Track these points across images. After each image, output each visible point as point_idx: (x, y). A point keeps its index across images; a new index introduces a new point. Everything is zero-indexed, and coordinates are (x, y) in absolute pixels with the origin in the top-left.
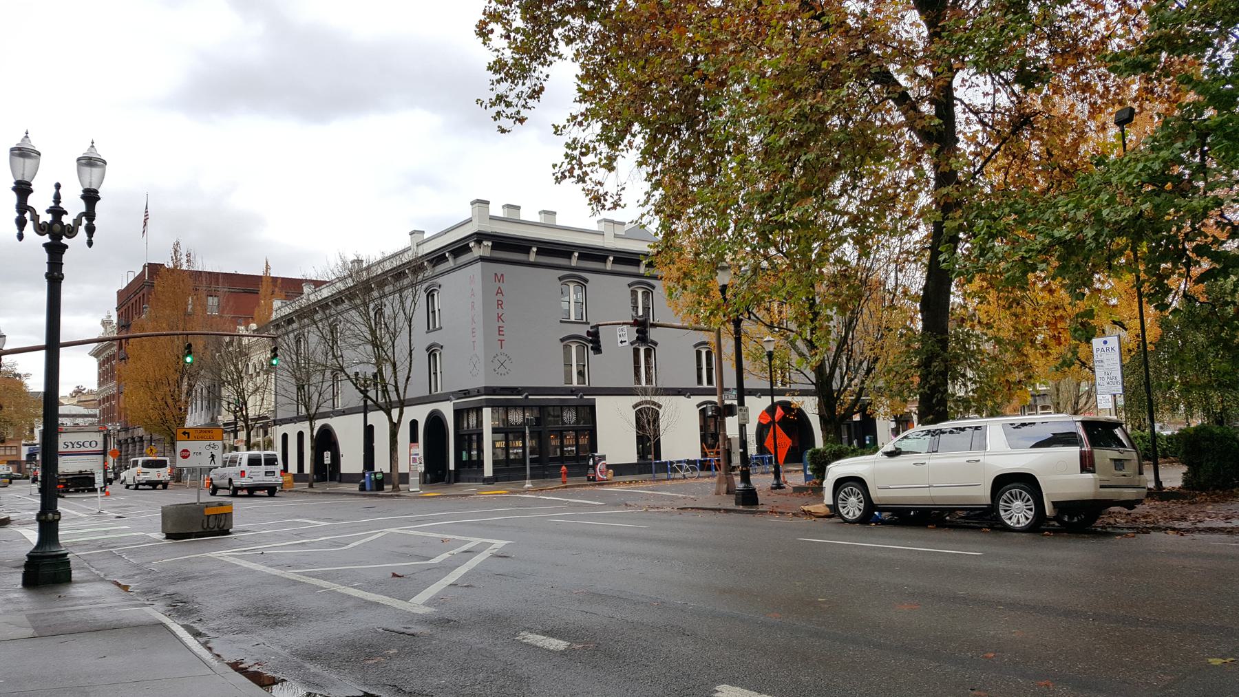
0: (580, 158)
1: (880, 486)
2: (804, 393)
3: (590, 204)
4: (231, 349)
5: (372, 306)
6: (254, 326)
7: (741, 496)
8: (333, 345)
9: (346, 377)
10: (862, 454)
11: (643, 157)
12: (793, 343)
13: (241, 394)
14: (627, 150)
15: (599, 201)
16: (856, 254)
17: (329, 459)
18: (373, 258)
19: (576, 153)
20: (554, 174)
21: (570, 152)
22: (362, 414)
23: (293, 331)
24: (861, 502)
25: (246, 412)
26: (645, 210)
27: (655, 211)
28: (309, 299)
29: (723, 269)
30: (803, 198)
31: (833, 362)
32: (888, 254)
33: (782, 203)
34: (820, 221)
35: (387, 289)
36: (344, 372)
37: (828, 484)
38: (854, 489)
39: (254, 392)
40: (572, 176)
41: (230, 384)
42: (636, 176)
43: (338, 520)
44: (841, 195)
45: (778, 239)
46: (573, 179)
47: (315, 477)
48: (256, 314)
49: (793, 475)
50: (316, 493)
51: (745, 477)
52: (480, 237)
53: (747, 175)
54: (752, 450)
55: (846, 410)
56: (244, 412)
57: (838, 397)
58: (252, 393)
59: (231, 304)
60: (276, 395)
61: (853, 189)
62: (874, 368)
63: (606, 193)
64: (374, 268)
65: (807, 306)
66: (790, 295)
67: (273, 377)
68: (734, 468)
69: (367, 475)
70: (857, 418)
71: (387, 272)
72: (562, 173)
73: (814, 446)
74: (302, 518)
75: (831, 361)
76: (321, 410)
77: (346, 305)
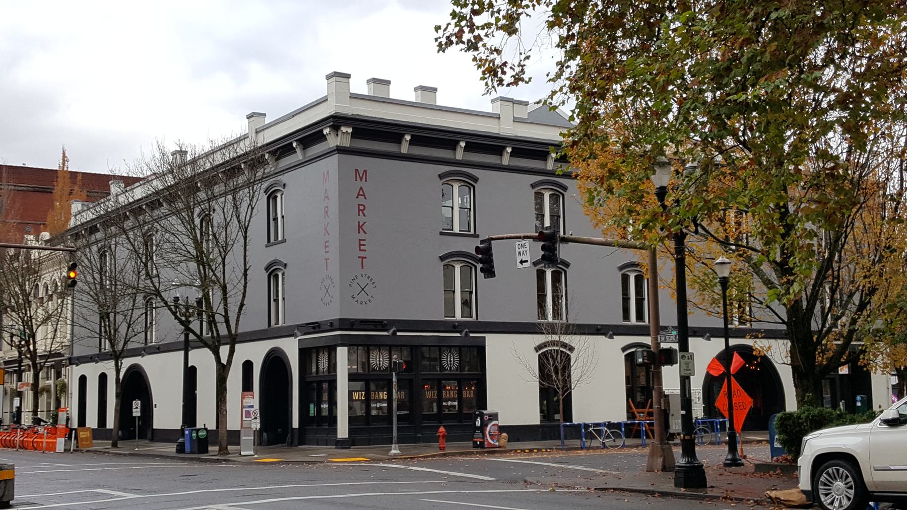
0: (471, 18)
1: (877, 466)
2: (771, 335)
3: (483, 79)
4: (15, 265)
5: (197, 210)
6: (46, 235)
7: (682, 475)
8: (147, 261)
9: (162, 304)
10: (852, 422)
11: (555, 15)
12: (756, 267)
13: (28, 323)
14: (534, 6)
15: (496, 75)
16: (845, 145)
17: (139, 410)
18: (201, 148)
19: (467, 11)
20: (436, 40)
21: (458, 10)
22: (182, 352)
23: (97, 242)
24: (851, 488)
25: (34, 347)
26: (556, 86)
27: (570, 87)
28: (117, 202)
29: (663, 165)
30: (773, 69)
31: (812, 294)
32: (890, 147)
33: (744, 77)
34: (796, 100)
35: (217, 189)
36: (161, 297)
37: (805, 462)
38: (841, 470)
39: (45, 321)
40: (460, 41)
41: (13, 310)
42: (545, 41)
43: (149, 492)
44: (825, 65)
45: (737, 125)
46: (461, 46)
47: (120, 433)
48: (49, 219)
49: (756, 447)
50: (120, 454)
51: (689, 449)
52: (337, 121)
53: (696, 39)
54: (698, 411)
55: (830, 360)
56: (31, 347)
57: (819, 342)
58: (42, 323)
59: (17, 205)
60: (72, 325)
61: (843, 57)
62: (869, 302)
63: (505, 64)
64: (201, 162)
65: (777, 216)
66: (755, 202)
67: (70, 302)
68: (672, 436)
69: (187, 432)
70: (844, 370)
71: (217, 166)
72: (448, 38)
73: (785, 410)
74: (103, 487)
75: (809, 291)
76: (130, 346)
77: (165, 209)
